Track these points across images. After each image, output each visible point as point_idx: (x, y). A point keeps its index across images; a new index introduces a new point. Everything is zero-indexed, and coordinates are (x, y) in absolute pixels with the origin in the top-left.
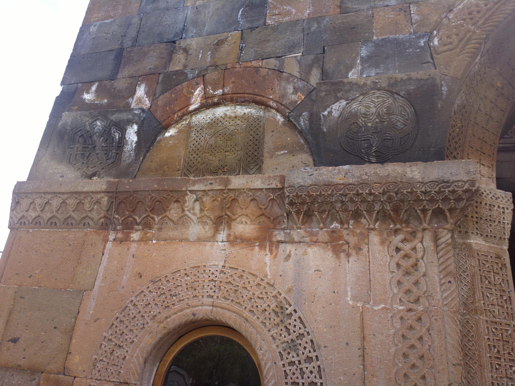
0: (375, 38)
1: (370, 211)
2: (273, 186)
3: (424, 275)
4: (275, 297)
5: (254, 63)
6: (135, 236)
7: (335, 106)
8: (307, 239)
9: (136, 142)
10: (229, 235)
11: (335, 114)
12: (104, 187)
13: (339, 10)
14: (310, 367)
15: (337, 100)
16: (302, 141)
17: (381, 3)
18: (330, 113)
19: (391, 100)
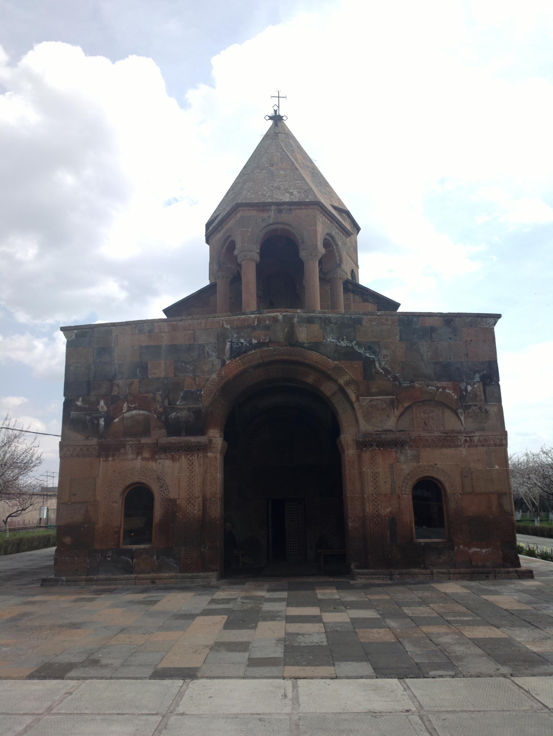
0: (185, 389)
1: (182, 449)
2: (154, 442)
3: (195, 465)
4: (157, 475)
5: (145, 395)
6: (110, 459)
7: (173, 414)
8: (165, 458)
9: (104, 425)
10: (141, 458)
11: (173, 417)
12: (96, 443)
13: (174, 375)
14: (166, 491)
15: (173, 412)
16: (163, 425)
17: (187, 375)
18: (171, 416)
19: (189, 413)
